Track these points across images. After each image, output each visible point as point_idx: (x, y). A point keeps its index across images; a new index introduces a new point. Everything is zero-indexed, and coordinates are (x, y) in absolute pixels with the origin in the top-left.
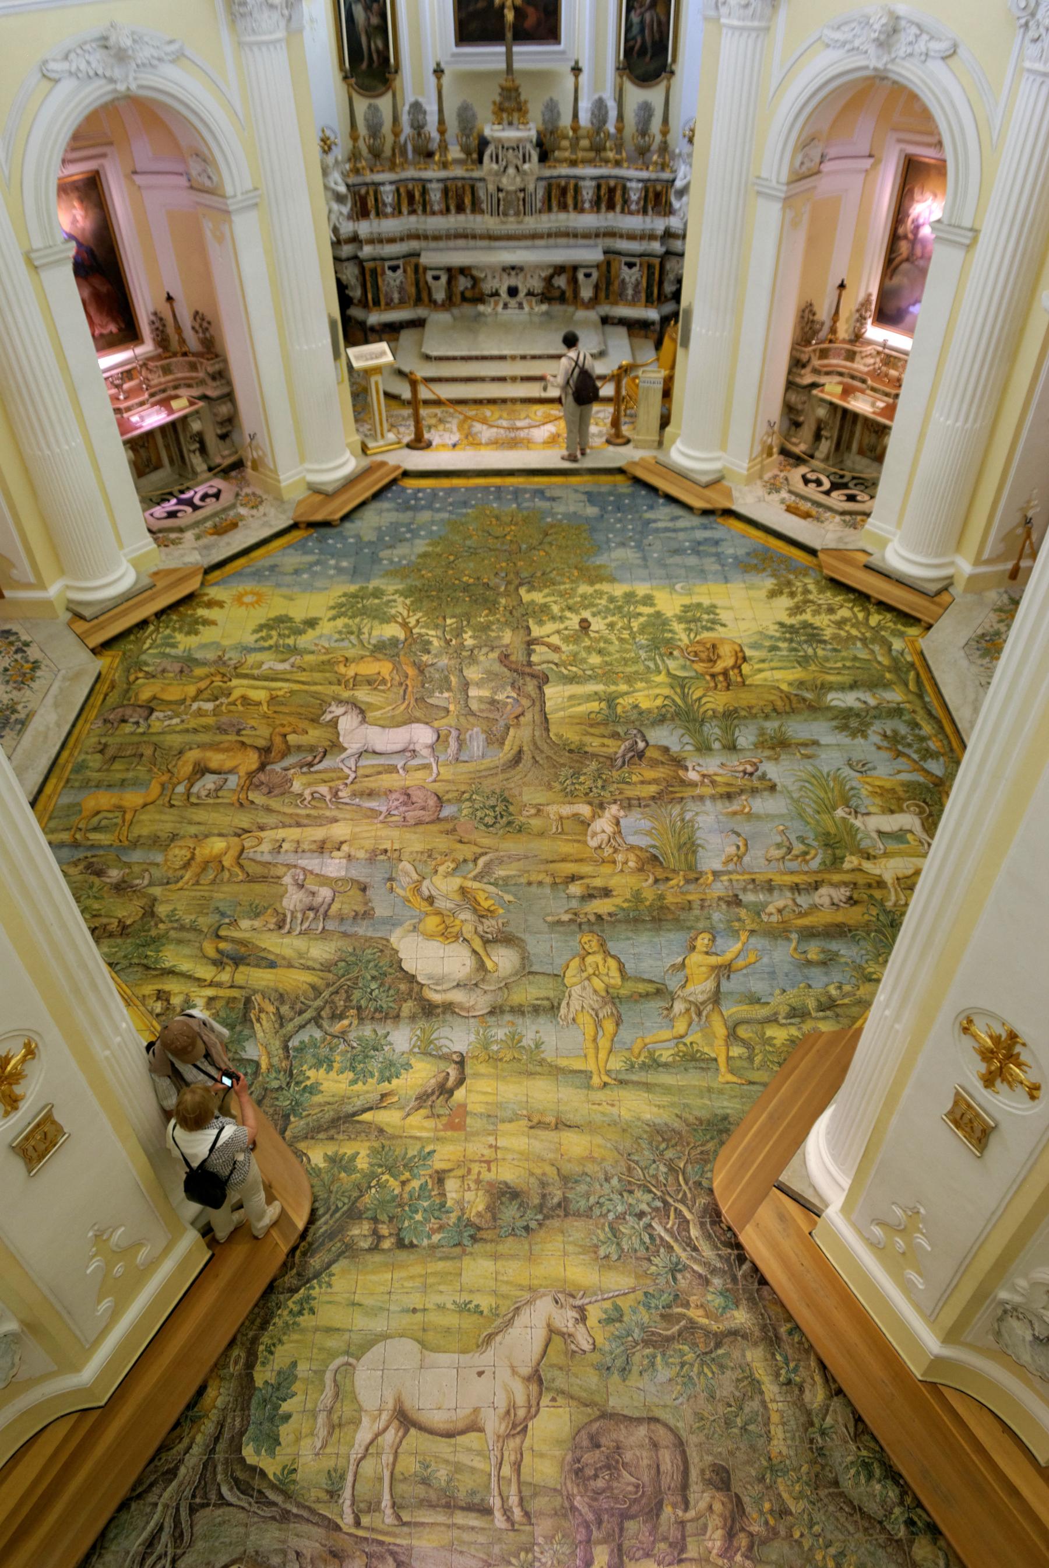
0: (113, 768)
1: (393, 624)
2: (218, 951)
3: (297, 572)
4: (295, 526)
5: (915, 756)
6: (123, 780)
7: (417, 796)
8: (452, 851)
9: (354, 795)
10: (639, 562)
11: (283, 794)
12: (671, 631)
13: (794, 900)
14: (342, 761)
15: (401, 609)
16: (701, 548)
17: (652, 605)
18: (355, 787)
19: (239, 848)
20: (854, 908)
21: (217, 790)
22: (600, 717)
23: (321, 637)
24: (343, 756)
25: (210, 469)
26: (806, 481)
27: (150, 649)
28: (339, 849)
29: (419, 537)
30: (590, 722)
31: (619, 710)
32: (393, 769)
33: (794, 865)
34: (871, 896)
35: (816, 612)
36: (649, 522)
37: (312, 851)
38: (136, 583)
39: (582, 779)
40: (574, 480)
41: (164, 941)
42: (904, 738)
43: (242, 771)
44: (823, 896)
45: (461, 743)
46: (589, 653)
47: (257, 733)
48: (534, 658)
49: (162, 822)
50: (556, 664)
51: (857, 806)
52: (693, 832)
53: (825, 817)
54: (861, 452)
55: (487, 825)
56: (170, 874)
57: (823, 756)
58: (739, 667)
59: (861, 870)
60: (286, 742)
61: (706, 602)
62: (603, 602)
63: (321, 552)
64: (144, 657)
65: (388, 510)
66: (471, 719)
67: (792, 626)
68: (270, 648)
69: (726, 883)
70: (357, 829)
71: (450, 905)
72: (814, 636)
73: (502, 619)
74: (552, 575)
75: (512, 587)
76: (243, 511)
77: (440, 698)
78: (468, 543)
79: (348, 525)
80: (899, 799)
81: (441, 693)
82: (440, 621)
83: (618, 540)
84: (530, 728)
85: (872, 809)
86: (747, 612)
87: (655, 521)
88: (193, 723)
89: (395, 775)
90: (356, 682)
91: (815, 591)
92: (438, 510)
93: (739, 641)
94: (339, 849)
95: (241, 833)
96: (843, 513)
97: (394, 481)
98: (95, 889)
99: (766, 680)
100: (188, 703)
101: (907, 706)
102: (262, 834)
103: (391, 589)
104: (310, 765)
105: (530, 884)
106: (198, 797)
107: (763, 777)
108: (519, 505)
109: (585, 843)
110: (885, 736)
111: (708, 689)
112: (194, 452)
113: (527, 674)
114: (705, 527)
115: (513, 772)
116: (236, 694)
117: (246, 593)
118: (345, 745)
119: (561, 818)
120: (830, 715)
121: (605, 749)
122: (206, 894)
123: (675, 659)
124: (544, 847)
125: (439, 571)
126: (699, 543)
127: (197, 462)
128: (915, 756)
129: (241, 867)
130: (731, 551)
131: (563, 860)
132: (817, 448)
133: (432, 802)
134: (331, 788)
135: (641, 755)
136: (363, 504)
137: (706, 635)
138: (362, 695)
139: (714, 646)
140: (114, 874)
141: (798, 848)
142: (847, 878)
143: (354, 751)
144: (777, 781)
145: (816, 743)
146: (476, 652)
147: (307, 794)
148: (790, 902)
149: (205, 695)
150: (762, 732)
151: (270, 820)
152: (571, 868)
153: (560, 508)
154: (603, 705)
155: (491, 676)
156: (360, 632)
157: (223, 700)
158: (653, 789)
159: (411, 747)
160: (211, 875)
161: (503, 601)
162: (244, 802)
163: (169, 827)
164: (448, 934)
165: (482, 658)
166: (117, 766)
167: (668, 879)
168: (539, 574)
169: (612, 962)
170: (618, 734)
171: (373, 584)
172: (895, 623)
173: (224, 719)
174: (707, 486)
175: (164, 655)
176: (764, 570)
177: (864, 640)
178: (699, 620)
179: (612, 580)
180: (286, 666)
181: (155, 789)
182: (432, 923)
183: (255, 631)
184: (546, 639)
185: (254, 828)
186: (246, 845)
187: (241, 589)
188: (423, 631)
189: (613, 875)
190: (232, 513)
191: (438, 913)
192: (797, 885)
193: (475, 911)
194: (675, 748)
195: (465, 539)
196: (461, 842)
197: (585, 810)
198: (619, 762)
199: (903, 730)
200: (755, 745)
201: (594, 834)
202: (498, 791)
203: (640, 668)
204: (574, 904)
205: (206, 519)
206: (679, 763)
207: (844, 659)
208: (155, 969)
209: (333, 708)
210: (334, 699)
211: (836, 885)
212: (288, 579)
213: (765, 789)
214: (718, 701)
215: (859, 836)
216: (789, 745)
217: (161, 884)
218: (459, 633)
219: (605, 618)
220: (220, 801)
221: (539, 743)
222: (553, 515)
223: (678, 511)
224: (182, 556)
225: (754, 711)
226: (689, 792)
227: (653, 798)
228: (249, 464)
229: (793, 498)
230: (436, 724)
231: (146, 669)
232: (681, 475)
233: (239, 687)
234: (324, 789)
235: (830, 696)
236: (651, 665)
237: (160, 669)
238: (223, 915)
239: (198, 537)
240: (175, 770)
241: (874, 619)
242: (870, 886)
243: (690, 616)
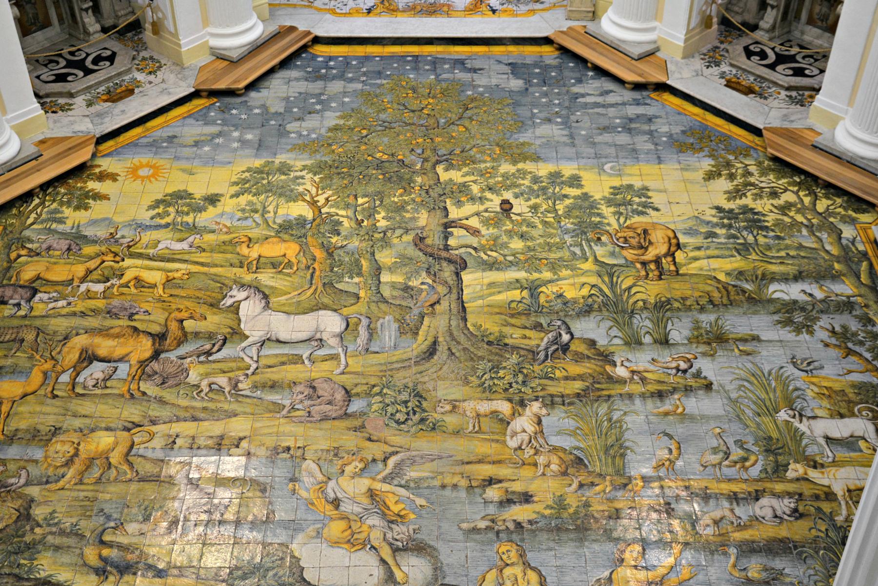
1: (300, 203)
2: (100, 557)
3: (196, 144)
4: (196, 94)
5: (868, 356)
7: (324, 390)
8: (360, 450)
9: (255, 387)
10: (565, 139)
11: (177, 385)
12: (599, 215)
13: (732, 510)
14: (243, 350)
15: (309, 187)
16: (633, 126)
17: (580, 186)
18: (256, 378)
19: (129, 444)
20: (800, 522)
21: (105, 380)
22: (521, 307)
23: (222, 215)
24: (244, 344)
25: (104, 30)
26: (749, 53)
27: (34, 224)
28: (237, 446)
29: (330, 109)
30: (510, 312)
31: (542, 299)
32: (297, 360)
33: (731, 472)
34: (819, 509)
35: (758, 196)
36: (577, 96)
37: (207, 447)
39: (501, 373)
40: (497, 49)
41: (40, 547)
42: (855, 334)
43: (134, 359)
44: (765, 507)
45: (372, 332)
46: (511, 237)
47: (152, 318)
48: (452, 242)
50: (475, 249)
51: (802, 409)
52: (622, 433)
53: (767, 420)
54: (811, 22)
55: (398, 422)
56: (50, 472)
57: (764, 353)
58: (673, 254)
59: (807, 480)
60: (183, 328)
61: (638, 184)
62: (527, 182)
63: (225, 123)
64: (27, 233)
65: (297, 79)
66: (383, 306)
67: (731, 211)
68: (167, 225)
69: (657, 491)
70: (258, 425)
71: (357, 509)
72: (755, 222)
73: (418, 199)
74: (472, 153)
75: (428, 165)
76: (140, 76)
77: (349, 284)
78: (383, 116)
79: (253, 94)
80: (849, 402)
81: (352, 278)
82: (351, 200)
83: (542, 115)
84: (447, 317)
85: (819, 413)
86: (683, 195)
87: (583, 96)
88: (80, 306)
89: (299, 366)
90: (259, 264)
91: (756, 173)
92: (351, 80)
93: (672, 227)
94: (237, 446)
95: (130, 427)
96: (788, 89)
97: (304, 48)
99: (701, 269)
100: (75, 284)
101: (859, 299)
102: (154, 428)
103: (299, 164)
104: (209, 353)
105: (443, 487)
106: (85, 387)
107: (698, 375)
108: (437, 76)
109: (504, 443)
110: (833, 332)
111: (638, 278)
112: (86, 10)
113: (444, 260)
114: (637, 103)
115: (427, 365)
116: (129, 275)
117: (142, 166)
118: (247, 333)
119: (478, 415)
120: (772, 309)
121: (526, 342)
122: (90, 494)
123: (604, 245)
124: (459, 447)
125: (350, 146)
126: (631, 120)
127: (90, 22)
128: (868, 356)
129: (131, 465)
130: (665, 129)
131: (480, 462)
132: (762, 18)
133: (340, 395)
134: (230, 379)
135: (565, 348)
136: (271, 71)
137: (636, 219)
138: (266, 278)
139: (645, 232)
141: (737, 453)
142: (791, 487)
143: (256, 339)
144: (711, 377)
145: (756, 338)
146: (389, 234)
147: (204, 384)
148: (727, 513)
149: (95, 276)
150: (697, 326)
151: (165, 413)
152: (487, 470)
153: (481, 80)
154: (525, 293)
155: (404, 260)
156: (265, 211)
157: (114, 281)
158: (578, 386)
159: (318, 336)
160: (96, 473)
161: (419, 180)
162: (137, 394)
163: (51, 420)
164: (355, 542)
165: (395, 241)
167: (593, 484)
168: (457, 151)
169: (533, 576)
170: (541, 325)
171: (280, 158)
172: (845, 209)
173: (115, 302)
174: (639, 59)
175: (50, 231)
176: (701, 149)
177: (810, 227)
178: (630, 203)
179: (537, 159)
180: (184, 245)
181: (36, 377)
182: (336, 528)
183: (151, 207)
184: (465, 222)
186: (137, 440)
187: (136, 161)
188: (333, 210)
189: (535, 478)
190: (127, 78)
191: (344, 518)
192: (735, 494)
193: (384, 515)
194: (602, 342)
195: (379, 112)
196: (370, 439)
197: (505, 407)
198: (542, 356)
199: (854, 326)
200: (689, 339)
201: (514, 434)
202: (410, 385)
203: (566, 254)
204: (492, 509)
205: (99, 84)
206: (606, 358)
207: (787, 247)
208: (28, 580)
209: (234, 292)
210: (235, 282)
211: (778, 496)
212: (187, 152)
213: (700, 388)
214: (651, 290)
215: (804, 442)
216: (727, 341)
217: (40, 484)
218: (371, 213)
219: (529, 199)
221: (455, 333)
222: (475, 87)
223: (609, 85)
224: (72, 123)
225: (688, 303)
226: (617, 390)
227: (578, 395)
228: (148, 26)
229: (734, 72)
230: (345, 311)
231: (29, 246)
232: (614, 47)
233: (133, 268)
234: (222, 381)
235: (772, 287)
236: (577, 251)
237: (44, 246)
238: (108, 518)
239: (90, 104)
240: (60, 357)
241: (822, 205)
242: (817, 497)
243: (621, 198)
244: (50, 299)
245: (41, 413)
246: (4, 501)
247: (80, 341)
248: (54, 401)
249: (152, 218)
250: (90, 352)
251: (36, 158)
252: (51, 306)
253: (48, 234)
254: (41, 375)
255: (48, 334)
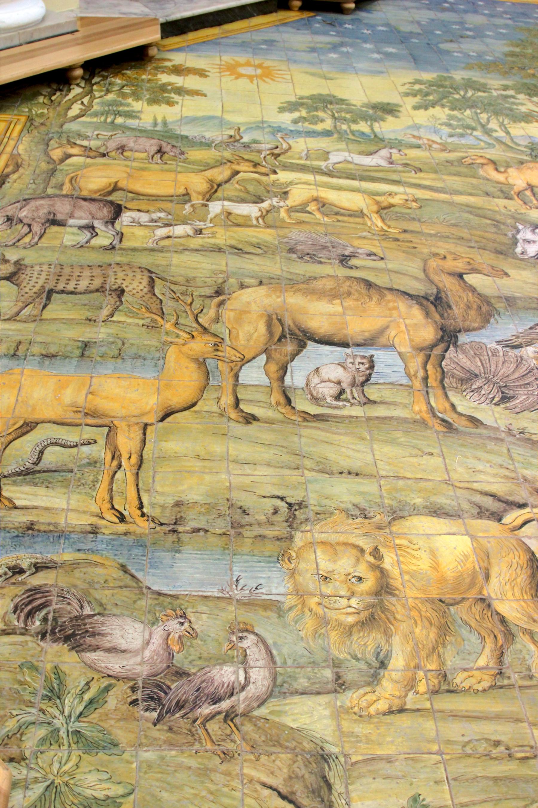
0: (47, 314)
6: (86, 345)
38: (43, 19)
49: (244, 467)
68: (327, 133)
88: (223, 237)
98: (72, 703)
100: (197, 200)
106: (316, 400)
140: (133, 642)
149: (230, 189)
166: (57, 309)
185: (522, 494)
220: (381, 411)
237: (112, 145)
240: (220, 329)
244: (152, 221)
245: (226, 458)
246: (227, 756)
247: (253, 302)
248: (252, 429)
249: (295, 122)
250: (288, 322)
251: (72, 32)
252: (162, 232)
253: (113, 130)
254: (193, 366)
255: (175, 283)
